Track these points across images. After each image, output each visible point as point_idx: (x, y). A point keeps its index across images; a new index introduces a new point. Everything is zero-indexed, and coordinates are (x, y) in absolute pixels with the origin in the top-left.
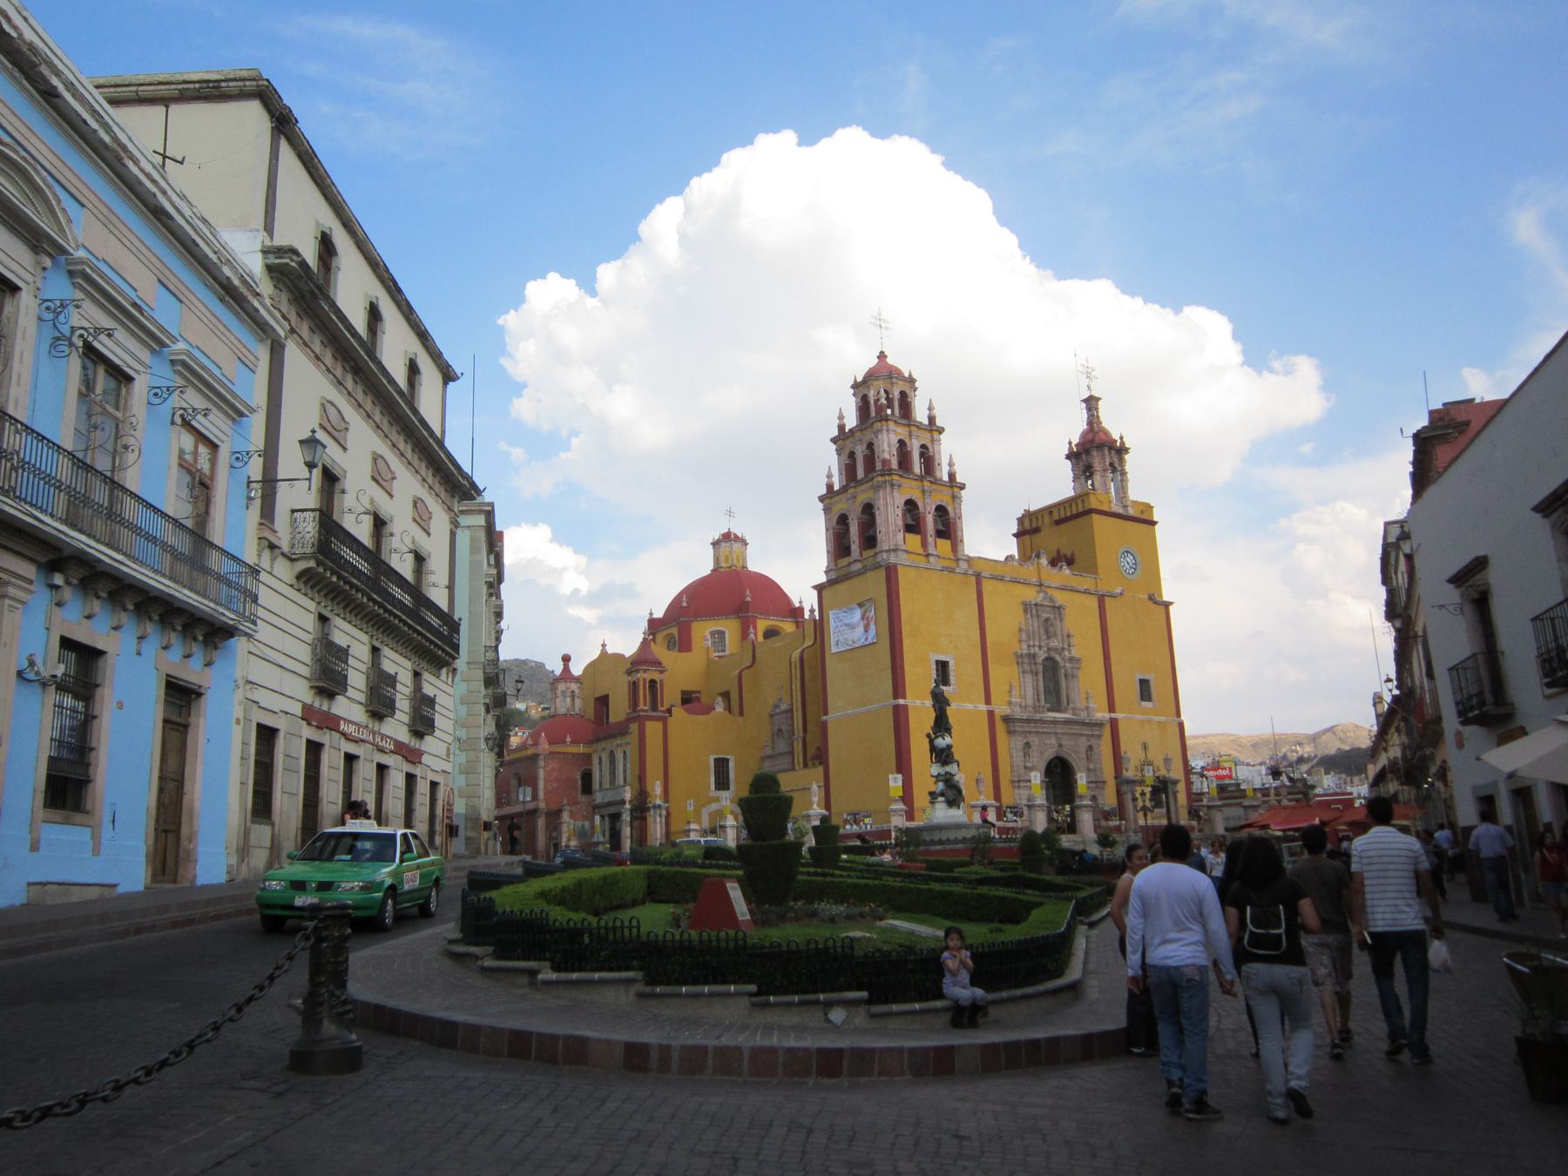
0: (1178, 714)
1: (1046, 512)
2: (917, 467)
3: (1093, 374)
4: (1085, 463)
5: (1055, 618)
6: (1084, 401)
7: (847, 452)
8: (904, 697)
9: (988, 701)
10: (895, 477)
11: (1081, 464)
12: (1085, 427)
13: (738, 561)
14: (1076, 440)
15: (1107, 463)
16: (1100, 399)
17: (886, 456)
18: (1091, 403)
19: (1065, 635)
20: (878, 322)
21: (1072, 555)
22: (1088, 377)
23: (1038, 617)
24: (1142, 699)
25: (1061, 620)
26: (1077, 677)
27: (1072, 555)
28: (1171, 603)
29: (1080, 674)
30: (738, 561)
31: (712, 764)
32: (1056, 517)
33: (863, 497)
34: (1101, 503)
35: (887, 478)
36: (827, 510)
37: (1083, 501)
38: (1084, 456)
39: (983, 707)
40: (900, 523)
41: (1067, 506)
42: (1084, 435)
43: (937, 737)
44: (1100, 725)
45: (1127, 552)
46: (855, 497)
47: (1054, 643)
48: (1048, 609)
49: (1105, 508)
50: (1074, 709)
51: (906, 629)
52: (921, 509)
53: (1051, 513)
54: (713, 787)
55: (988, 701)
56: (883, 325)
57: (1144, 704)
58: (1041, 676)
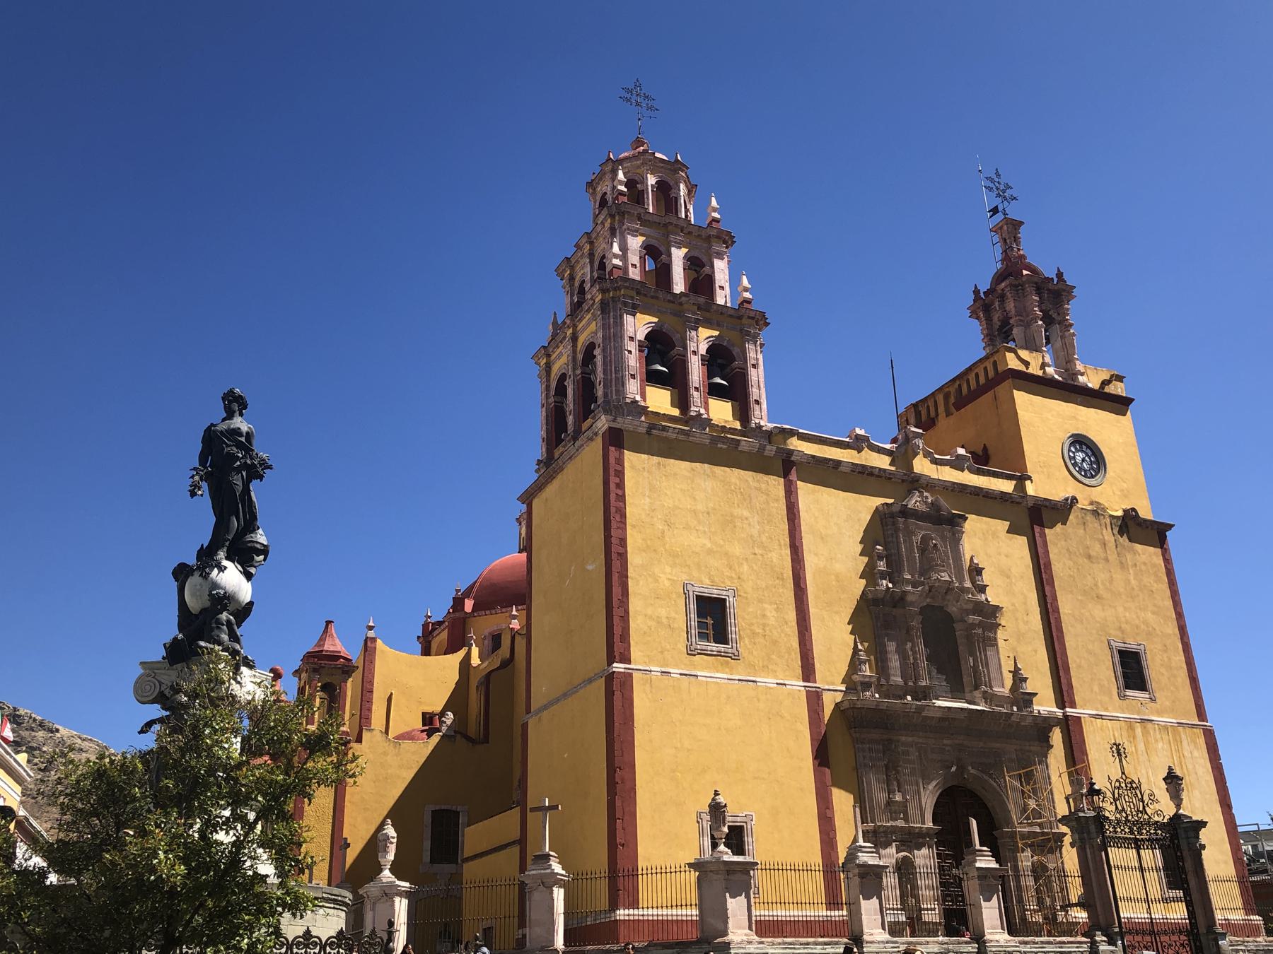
0: (1201, 714)
2: (679, 286)
7: (577, 284)
8: (626, 660)
9: (808, 672)
11: (996, 317)
12: (999, 266)
14: (984, 286)
18: (1010, 231)
21: (985, 449)
22: (998, 195)
24: (1128, 687)
26: (995, 639)
27: (985, 449)
28: (1170, 526)
29: (1000, 634)
31: (428, 819)
33: (582, 339)
34: (1027, 364)
37: (995, 363)
38: (997, 304)
39: (797, 685)
40: (633, 360)
41: (972, 377)
42: (999, 278)
44: (1043, 727)
45: (1081, 443)
46: (574, 339)
50: (989, 698)
51: (634, 540)
54: (427, 857)
55: (808, 672)
57: (1129, 693)
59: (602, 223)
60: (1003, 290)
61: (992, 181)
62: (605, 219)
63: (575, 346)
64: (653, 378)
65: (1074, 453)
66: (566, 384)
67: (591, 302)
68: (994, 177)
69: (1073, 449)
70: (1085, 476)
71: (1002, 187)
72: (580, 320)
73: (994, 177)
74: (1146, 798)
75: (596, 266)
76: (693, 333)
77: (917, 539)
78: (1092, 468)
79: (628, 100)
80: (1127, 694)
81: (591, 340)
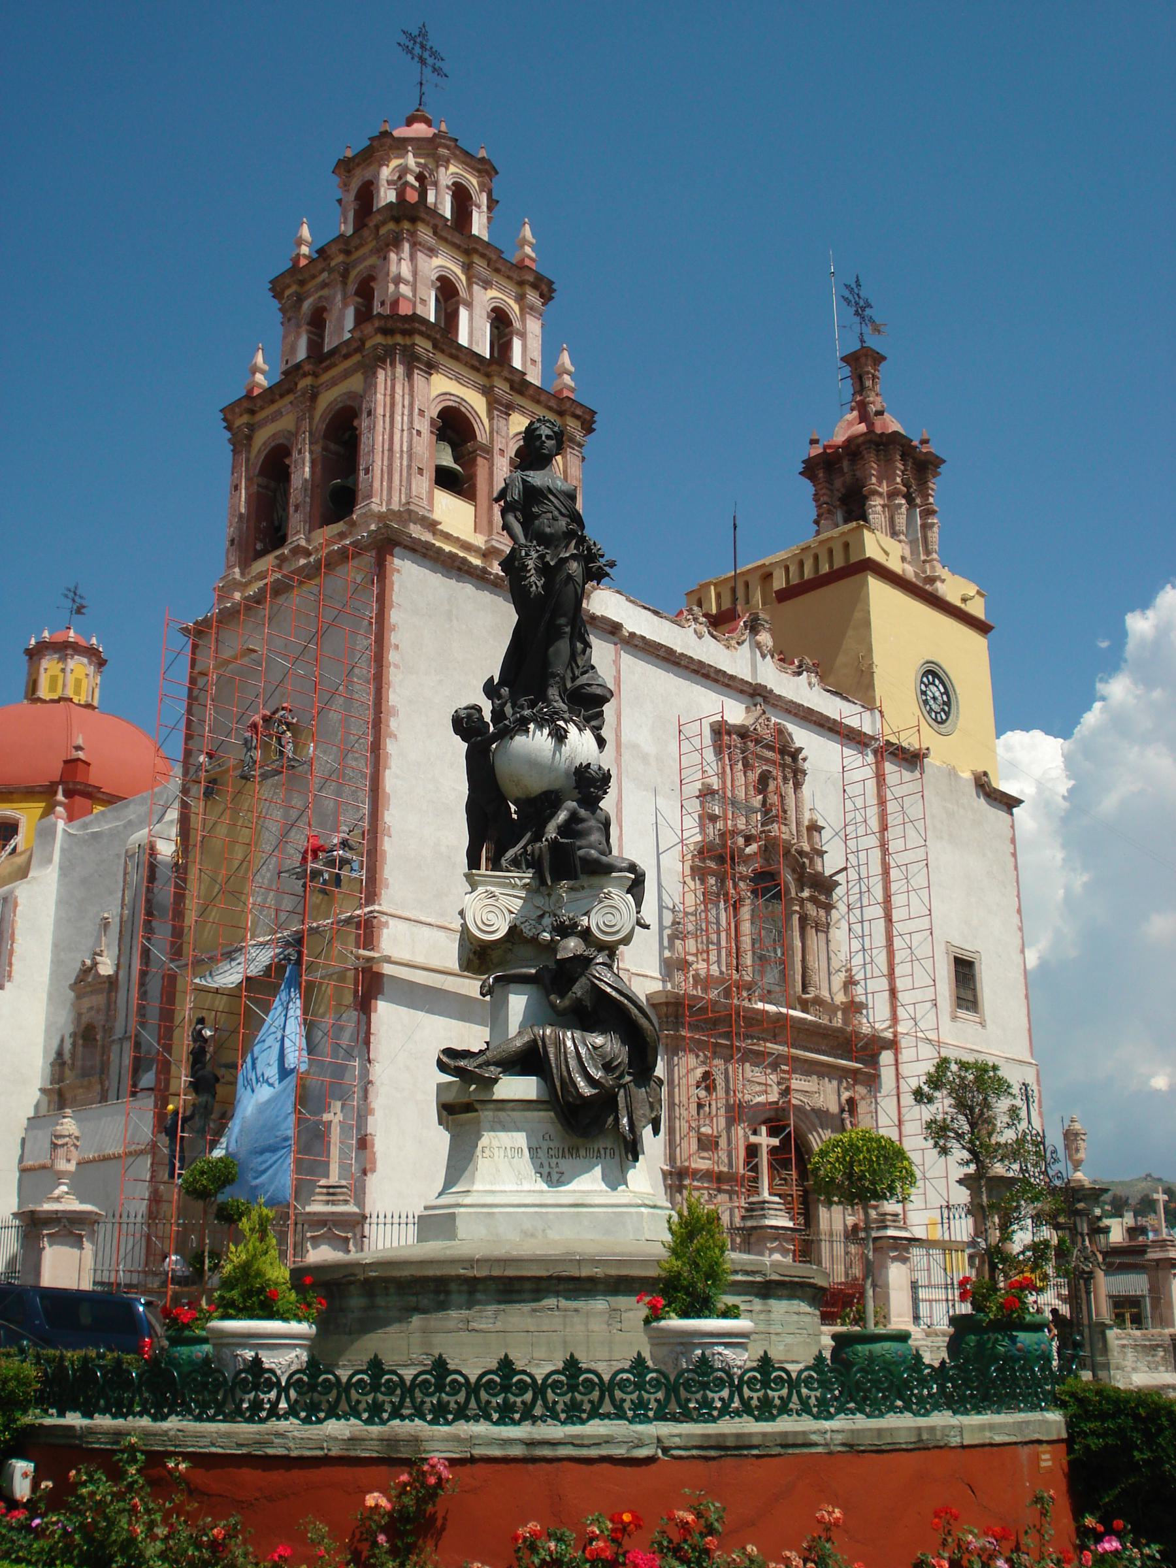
1: (759, 573)
3: (868, 312)
4: (848, 478)
5: (785, 779)
6: (848, 359)
10: (418, 340)
11: (838, 483)
13: (77, 693)
15: (898, 480)
16: (884, 358)
17: (405, 289)
19: (806, 823)
20: (418, 50)
22: (857, 313)
23: (747, 766)
24: (959, 1006)
25: (798, 785)
30: (77, 693)
32: (779, 583)
33: (328, 398)
34: (887, 554)
35: (399, 339)
36: (240, 441)
37: (846, 546)
38: (845, 464)
43: (522, 726)
46: (314, 397)
47: (782, 832)
48: (769, 754)
49: (895, 565)
52: (482, 437)
53: (767, 577)
56: (430, 61)
57: (961, 1013)
58: (745, 912)
59: (377, 228)
60: (859, 446)
61: (851, 291)
62: (384, 223)
63: (312, 409)
64: (446, 479)
65: (926, 686)
66: (287, 462)
67: (355, 345)
68: (854, 286)
69: (925, 680)
70: (935, 720)
71: (862, 303)
72: (328, 368)
73: (854, 286)
74: (1048, 1155)
75: (352, 288)
76: (503, 422)
77: (753, 776)
78: (943, 710)
79: (409, 51)
80: (959, 1015)
81: (349, 403)
